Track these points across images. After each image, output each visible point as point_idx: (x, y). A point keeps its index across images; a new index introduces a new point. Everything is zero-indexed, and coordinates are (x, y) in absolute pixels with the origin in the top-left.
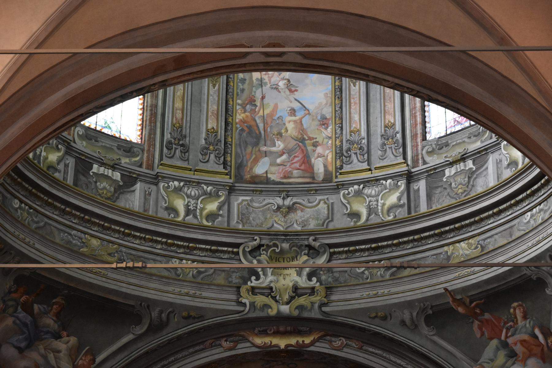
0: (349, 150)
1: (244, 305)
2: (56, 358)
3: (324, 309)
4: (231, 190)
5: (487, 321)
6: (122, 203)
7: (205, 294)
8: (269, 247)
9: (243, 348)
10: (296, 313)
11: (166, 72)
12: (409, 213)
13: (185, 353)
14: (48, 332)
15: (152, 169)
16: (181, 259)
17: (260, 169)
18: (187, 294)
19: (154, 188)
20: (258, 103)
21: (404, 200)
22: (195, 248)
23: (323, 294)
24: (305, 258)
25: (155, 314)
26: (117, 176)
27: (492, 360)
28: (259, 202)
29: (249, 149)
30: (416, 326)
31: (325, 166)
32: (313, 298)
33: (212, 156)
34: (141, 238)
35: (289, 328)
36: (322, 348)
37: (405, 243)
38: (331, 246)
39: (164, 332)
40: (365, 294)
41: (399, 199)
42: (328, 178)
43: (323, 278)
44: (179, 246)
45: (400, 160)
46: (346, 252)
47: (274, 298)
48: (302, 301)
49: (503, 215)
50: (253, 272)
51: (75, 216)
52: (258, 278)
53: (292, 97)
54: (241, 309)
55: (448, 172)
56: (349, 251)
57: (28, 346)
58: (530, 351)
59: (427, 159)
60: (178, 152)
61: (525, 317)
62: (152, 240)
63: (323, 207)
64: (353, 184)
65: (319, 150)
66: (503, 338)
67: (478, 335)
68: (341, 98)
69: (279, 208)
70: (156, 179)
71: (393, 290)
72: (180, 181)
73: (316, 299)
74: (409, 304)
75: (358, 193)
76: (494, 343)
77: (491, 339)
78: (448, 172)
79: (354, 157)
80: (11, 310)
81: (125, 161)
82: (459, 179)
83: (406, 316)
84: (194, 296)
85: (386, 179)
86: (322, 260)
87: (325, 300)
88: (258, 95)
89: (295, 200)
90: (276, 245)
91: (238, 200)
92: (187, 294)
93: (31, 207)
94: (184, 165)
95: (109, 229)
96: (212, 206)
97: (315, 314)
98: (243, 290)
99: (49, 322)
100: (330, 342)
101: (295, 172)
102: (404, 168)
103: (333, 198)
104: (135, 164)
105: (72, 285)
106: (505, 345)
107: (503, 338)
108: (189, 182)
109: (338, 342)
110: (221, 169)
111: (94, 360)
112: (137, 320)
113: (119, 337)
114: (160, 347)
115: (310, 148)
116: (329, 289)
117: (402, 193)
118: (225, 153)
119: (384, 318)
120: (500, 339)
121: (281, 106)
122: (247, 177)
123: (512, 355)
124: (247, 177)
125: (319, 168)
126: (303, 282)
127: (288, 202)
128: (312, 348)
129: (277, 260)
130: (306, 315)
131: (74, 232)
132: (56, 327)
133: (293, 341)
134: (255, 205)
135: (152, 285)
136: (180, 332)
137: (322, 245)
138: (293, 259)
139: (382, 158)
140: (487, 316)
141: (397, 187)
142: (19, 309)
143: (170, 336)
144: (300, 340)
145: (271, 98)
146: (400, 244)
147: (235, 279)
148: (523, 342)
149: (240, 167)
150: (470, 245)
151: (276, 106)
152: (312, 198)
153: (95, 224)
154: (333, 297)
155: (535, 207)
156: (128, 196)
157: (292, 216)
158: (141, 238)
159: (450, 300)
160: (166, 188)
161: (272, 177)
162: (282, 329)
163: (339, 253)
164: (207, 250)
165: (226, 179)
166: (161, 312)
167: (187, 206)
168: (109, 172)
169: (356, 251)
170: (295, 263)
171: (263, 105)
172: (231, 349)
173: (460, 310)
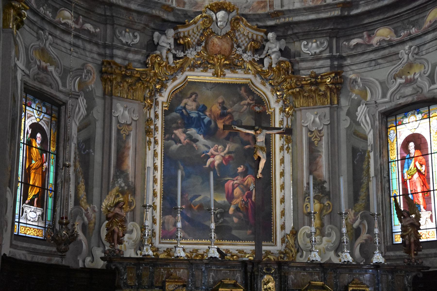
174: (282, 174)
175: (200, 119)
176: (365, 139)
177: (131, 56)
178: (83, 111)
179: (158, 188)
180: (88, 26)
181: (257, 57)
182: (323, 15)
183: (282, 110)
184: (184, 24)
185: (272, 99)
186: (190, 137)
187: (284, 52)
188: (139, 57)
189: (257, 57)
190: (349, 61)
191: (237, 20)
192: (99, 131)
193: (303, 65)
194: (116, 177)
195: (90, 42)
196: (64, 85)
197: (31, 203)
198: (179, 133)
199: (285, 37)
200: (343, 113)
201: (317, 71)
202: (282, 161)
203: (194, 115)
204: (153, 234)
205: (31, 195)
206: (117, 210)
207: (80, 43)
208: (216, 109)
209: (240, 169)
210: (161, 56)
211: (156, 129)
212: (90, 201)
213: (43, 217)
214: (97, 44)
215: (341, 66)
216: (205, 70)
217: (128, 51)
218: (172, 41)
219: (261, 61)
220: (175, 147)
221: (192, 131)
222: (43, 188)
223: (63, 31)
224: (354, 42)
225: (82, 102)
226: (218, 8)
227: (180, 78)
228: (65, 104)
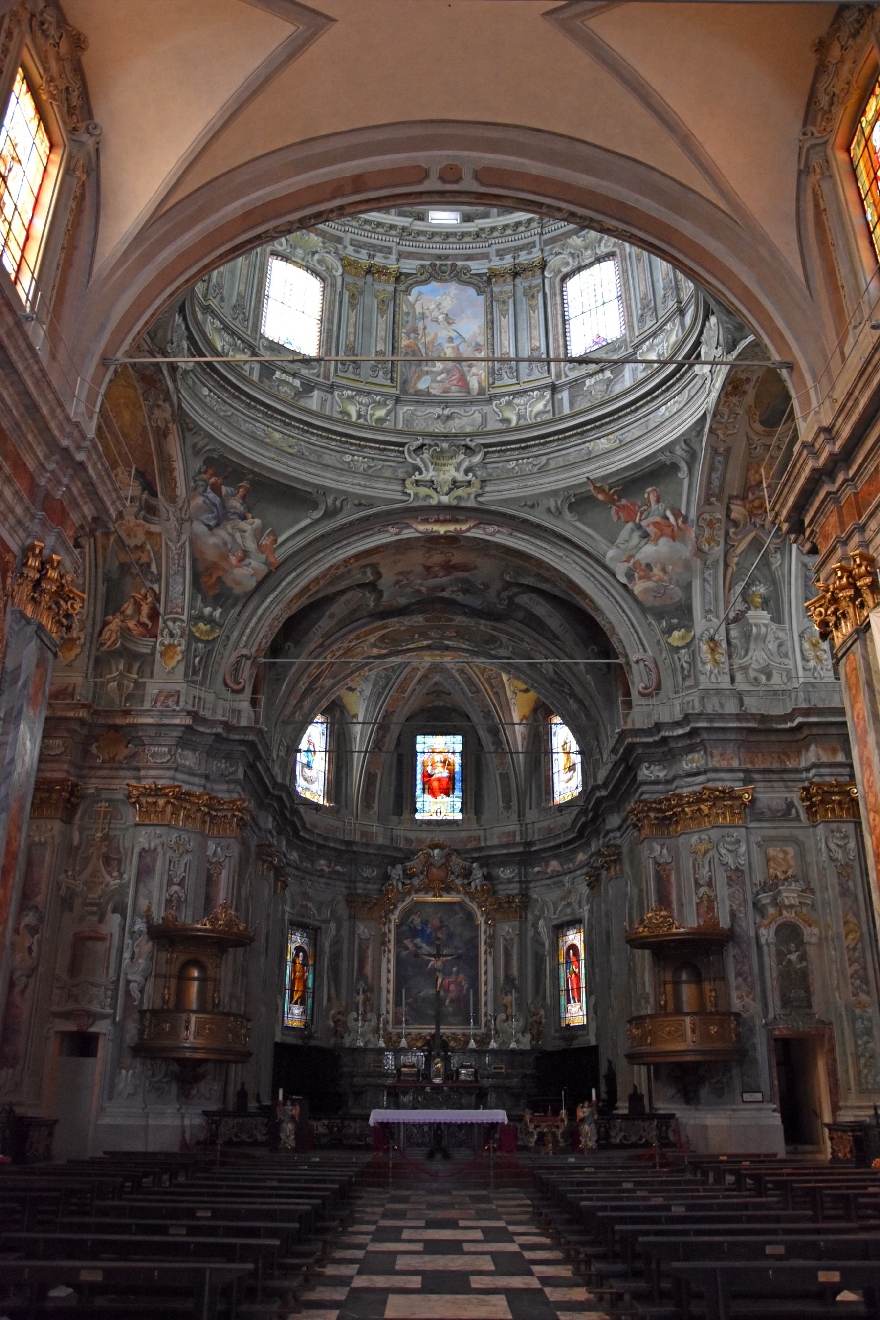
0: (500, 369)
1: (409, 495)
2: (242, 537)
3: (479, 499)
4: (397, 400)
5: (623, 506)
6: (303, 403)
7: (374, 485)
8: (430, 446)
9: (407, 534)
10: (454, 503)
11: (343, 195)
12: (554, 414)
13: (355, 538)
14: (235, 513)
15: (328, 379)
16: (353, 455)
17: (422, 385)
18: (359, 485)
19: (329, 396)
20: (421, 332)
21: (549, 407)
22: (366, 447)
23: (479, 486)
24: (463, 456)
25: (330, 501)
26: (297, 383)
27: (627, 541)
28: (422, 411)
29: (413, 368)
30: (560, 513)
31: (479, 383)
32: (469, 490)
33: (381, 373)
34: (318, 435)
35: (448, 517)
36: (477, 533)
37: (551, 442)
38: (485, 446)
39: (338, 517)
40: (515, 486)
41: (545, 406)
42: (482, 392)
43: (479, 473)
44: (351, 444)
45: (546, 375)
46: (498, 451)
47: (435, 490)
48: (459, 492)
49: (639, 412)
50: (417, 469)
51: (259, 411)
52: (421, 473)
53: (450, 328)
54: (406, 498)
55: (588, 382)
56: (501, 451)
57: (218, 525)
58: (661, 531)
59: (569, 373)
60: (351, 368)
61: (658, 501)
62: (328, 438)
63: (478, 417)
64: (503, 395)
65: (474, 370)
66: (637, 520)
67: (615, 519)
68: (493, 329)
69: (439, 416)
70: (331, 388)
71: (541, 481)
72: (353, 390)
73: (473, 490)
74: (555, 493)
75: (509, 403)
76: (630, 525)
77: (627, 522)
78: (588, 382)
79: (504, 374)
80: (201, 489)
81: (304, 372)
82: (598, 387)
83: (552, 504)
84: (365, 486)
85: (533, 391)
86: (477, 458)
87: (480, 492)
88: (420, 325)
89: (453, 410)
90: (436, 445)
91: (404, 410)
92: (359, 485)
93: (219, 397)
94: (357, 378)
95: (289, 425)
96: (381, 413)
97: (472, 503)
98: (408, 483)
99: (236, 504)
100: (484, 529)
101: (453, 388)
102: (549, 381)
103: (486, 409)
104: (313, 374)
105: (256, 470)
106: (639, 527)
107: (637, 520)
108: (360, 392)
109: (491, 529)
110: (388, 383)
111: (276, 540)
112: (315, 506)
113: (297, 521)
114: (334, 531)
115: (466, 369)
116: (484, 482)
117: (548, 401)
118: (392, 371)
119: (532, 507)
120: (634, 521)
121: (439, 335)
122: (412, 391)
123: (646, 536)
124: (412, 391)
125: (474, 384)
126: (460, 476)
127: (447, 412)
128: (468, 534)
129: (438, 458)
130: (463, 504)
131: (258, 425)
132: (242, 509)
133: (451, 528)
134: (419, 413)
135: (329, 475)
136: (352, 518)
137: (477, 445)
138: (452, 457)
139: (529, 375)
140: (624, 501)
141: (543, 397)
142: (209, 490)
143: (344, 521)
144: (458, 527)
145: (432, 329)
146: (546, 443)
147: (401, 474)
148: (655, 524)
149: (405, 382)
150: (609, 441)
151: (436, 335)
152: (468, 409)
153: (277, 419)
154: (487, 489)
155: (669, 400)
156: (307, 400)
157: (450, 423)
158: (318, 435)
159: (591, 488)
160: (340, 396)
161: (433, 391)
162: (441, 518)
163: (493, 452)
164: (376, 448)
165: (393, 391)
166: (335, 499)
167: (359, 412)
168: (290, 379)
169: (507, 450)
170: (454, 461)
171: (425, 335)
172: (397, 534)
173: (600, 497)
174: (486, 973)
175: (423, 931)
176: (543, 945)
177: (369, 886)
178: (334, 932)
179: (391, 987)
180: (338, 868)
181: (466, 882)
182: (512, 851)
183: (486, 922)
184: (409, 859)
185: (479, 914)
186: (416, 945)
187: (488, 877)
188: (376, 887)
189: (466, 882)
190: (532, 885)
191: (449, 855)
192: (345, 946)
193: (500, 887)
194: (358, 979)
195: (339, 880)
196: (319, 914)
197: (296, 1003)
198: (407, 942)
199: (487, 866)
200: (530, 924)
201: (509, 892)
202: (486, 963)
203: (419, 928)
204: (387, 1022)
205: (295, 998)
206: (340, 1017)
207: (331, 882)
208: (436, 922)
209: (454, 969)
210: (392, 885)
211: (389, 941)
212: (338, 998)
213: (304, 1012)
214: (344, 881)
215: (528, 888)
216: (427, 893)
217: (368, 883)
218: (401, 872)
219: (470, 884)
220: (404, 953)
221: (418, 940)
222: (304, 992)
223: (320, 876)
224: (537, 869)
225: (333, 925)
226: (434, 846)
227: (408, 900)
228: (320, 928)
